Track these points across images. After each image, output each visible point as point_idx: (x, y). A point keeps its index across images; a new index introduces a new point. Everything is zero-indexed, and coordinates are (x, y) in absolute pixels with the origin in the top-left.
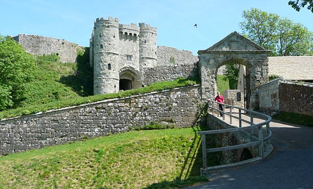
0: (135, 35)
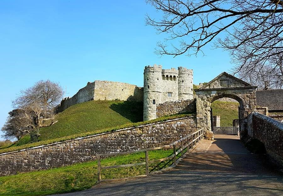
0: (175, 77)
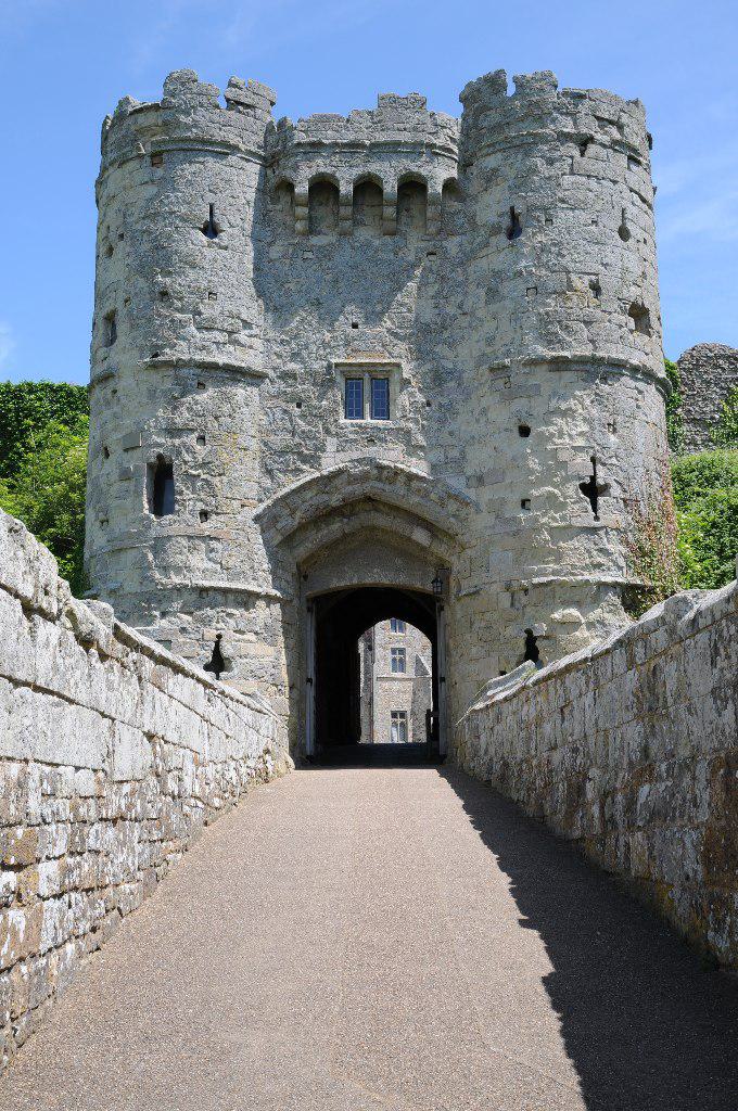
0: (413, 186)
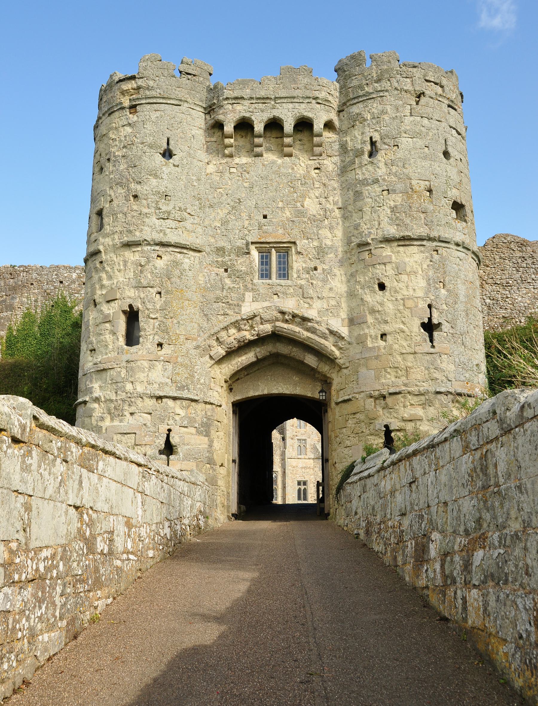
0: (304, 125)
